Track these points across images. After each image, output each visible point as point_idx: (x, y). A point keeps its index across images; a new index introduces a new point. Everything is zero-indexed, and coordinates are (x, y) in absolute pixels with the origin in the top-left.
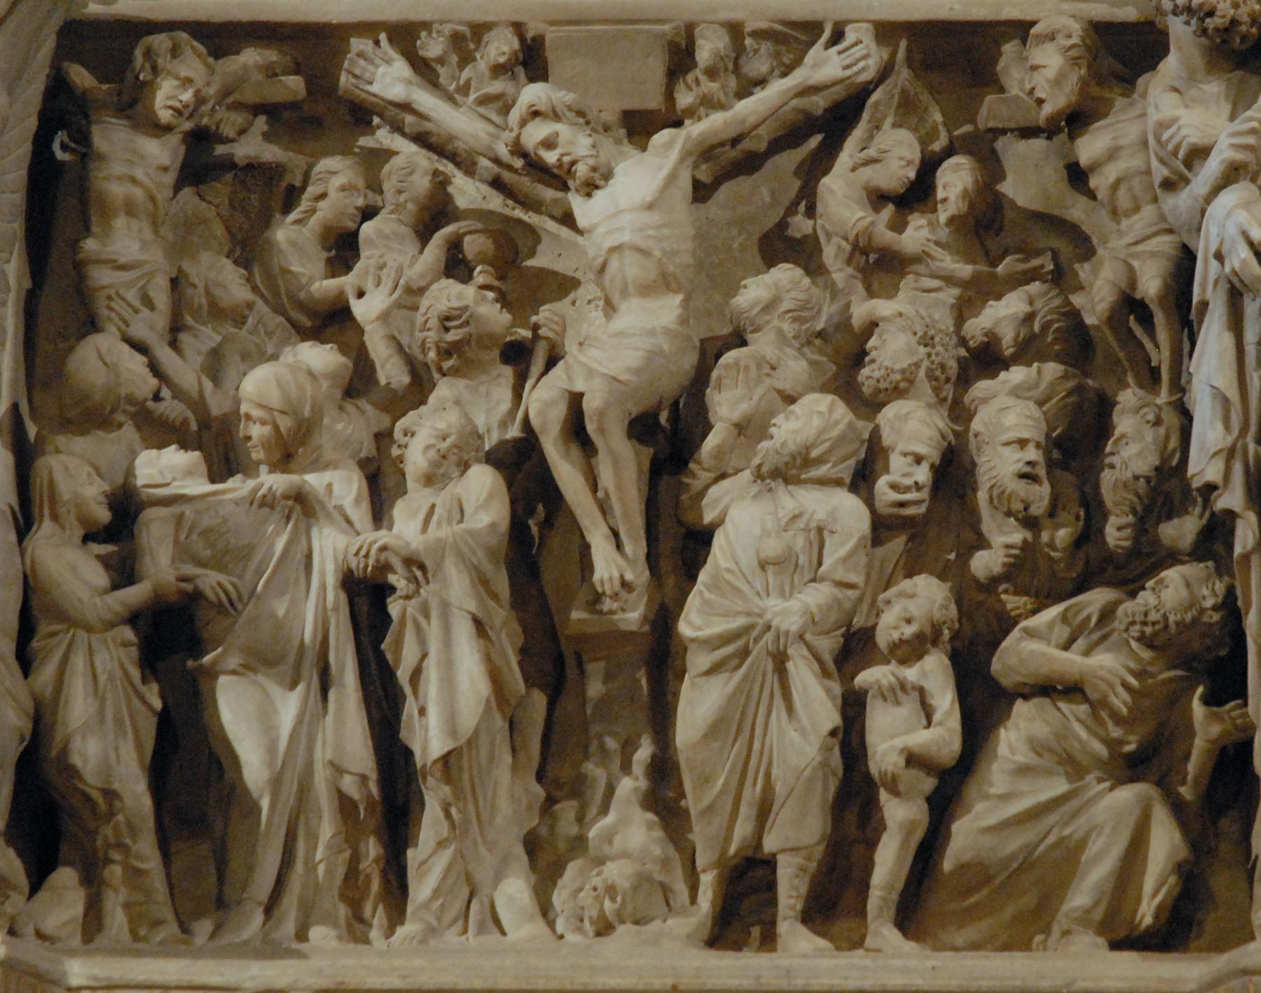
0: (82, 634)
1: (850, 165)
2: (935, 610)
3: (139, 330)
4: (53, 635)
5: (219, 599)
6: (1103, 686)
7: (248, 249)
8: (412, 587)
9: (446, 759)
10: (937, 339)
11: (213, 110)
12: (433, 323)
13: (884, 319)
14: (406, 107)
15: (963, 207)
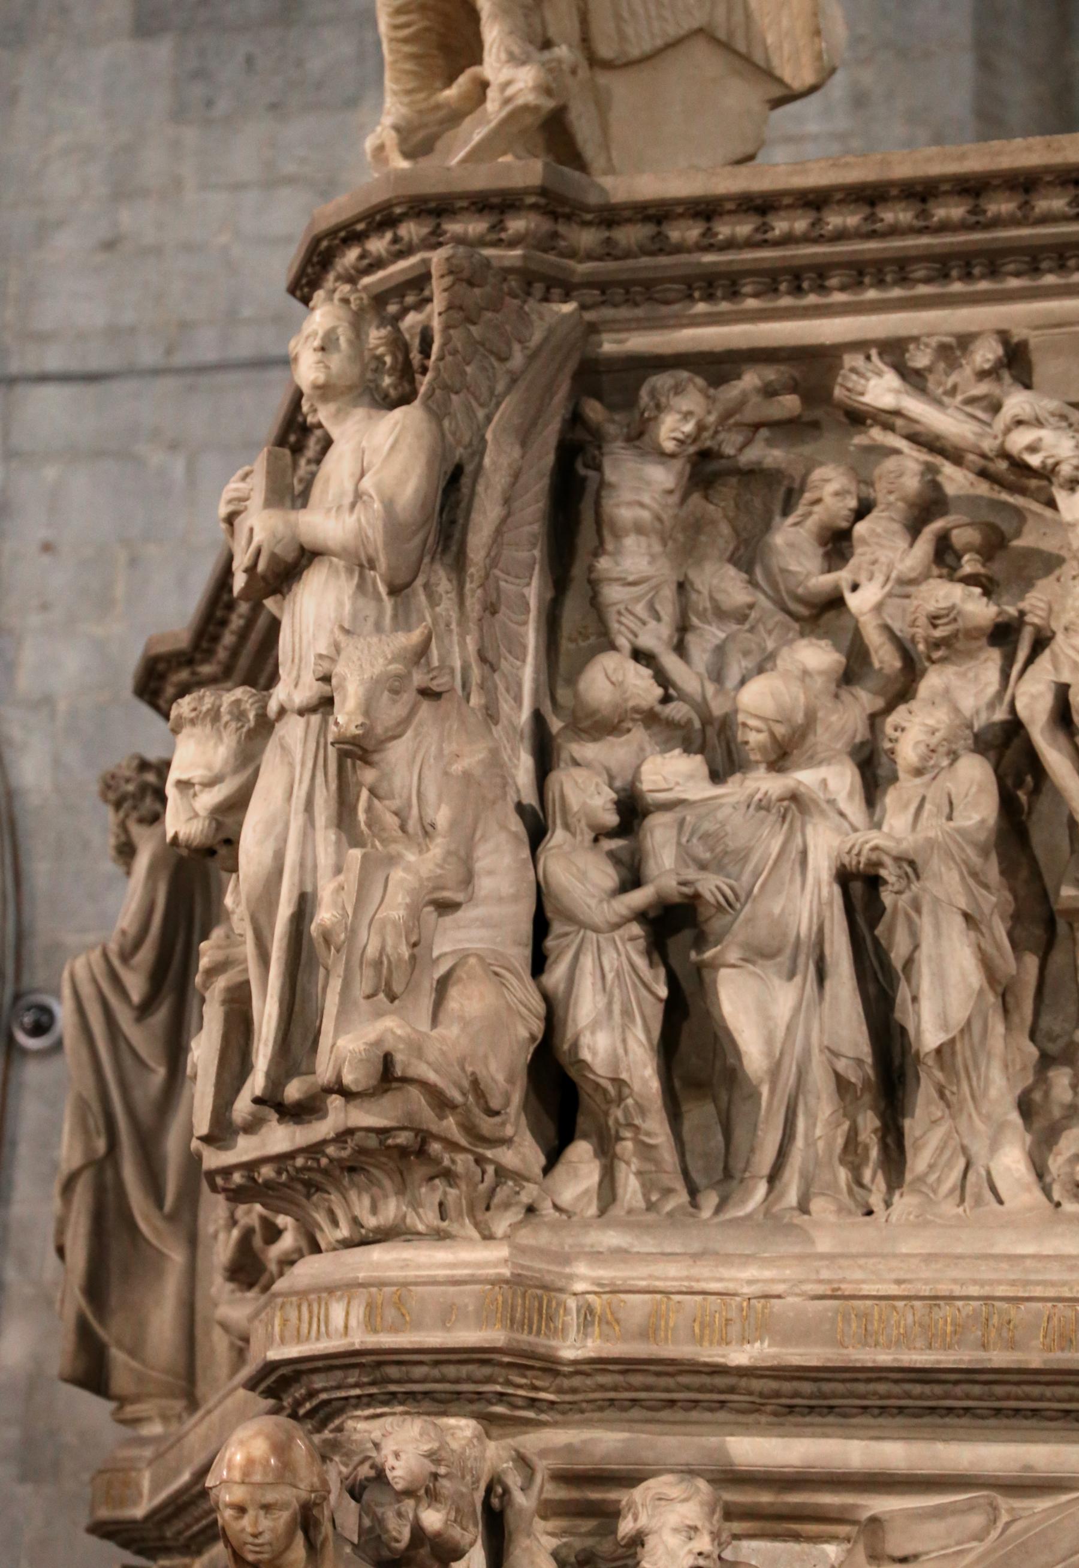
0: (589, 933)
3: (648, 641)
4: (566, 934)
5: (718, 902)
7: (748, 555)
8: (904, 882)
9: (939, 1051)
11: (716, 432)
12: (923, 621)
14: (897, 413)
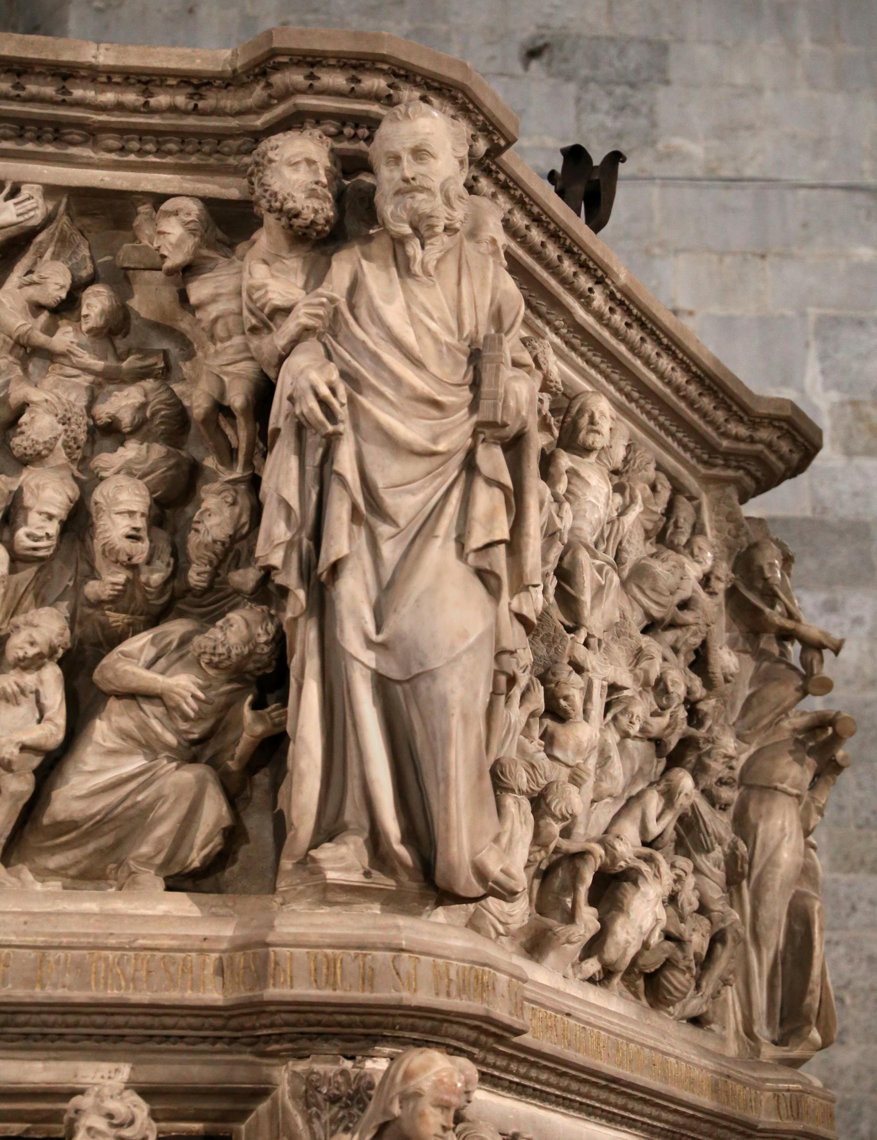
1: (18, 284)
2: (53, 637)
6: (177, 698)
10: (73, 420)
13: (33, 402)
15: (100, 322)
